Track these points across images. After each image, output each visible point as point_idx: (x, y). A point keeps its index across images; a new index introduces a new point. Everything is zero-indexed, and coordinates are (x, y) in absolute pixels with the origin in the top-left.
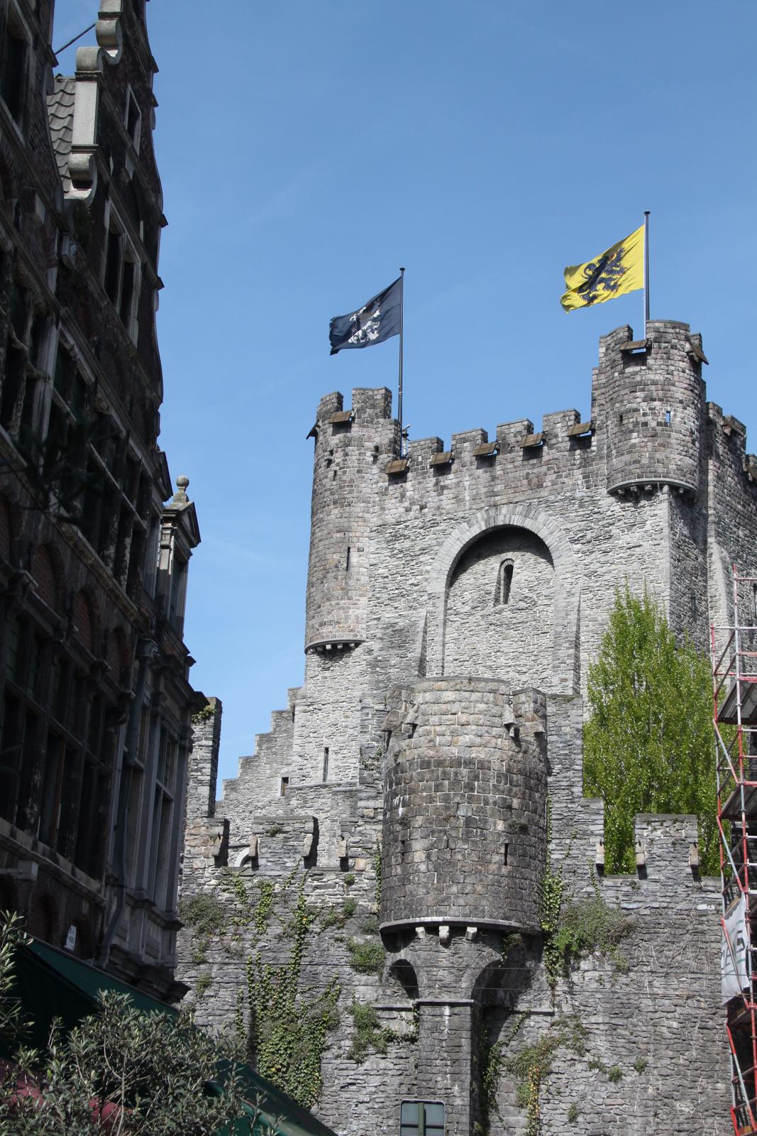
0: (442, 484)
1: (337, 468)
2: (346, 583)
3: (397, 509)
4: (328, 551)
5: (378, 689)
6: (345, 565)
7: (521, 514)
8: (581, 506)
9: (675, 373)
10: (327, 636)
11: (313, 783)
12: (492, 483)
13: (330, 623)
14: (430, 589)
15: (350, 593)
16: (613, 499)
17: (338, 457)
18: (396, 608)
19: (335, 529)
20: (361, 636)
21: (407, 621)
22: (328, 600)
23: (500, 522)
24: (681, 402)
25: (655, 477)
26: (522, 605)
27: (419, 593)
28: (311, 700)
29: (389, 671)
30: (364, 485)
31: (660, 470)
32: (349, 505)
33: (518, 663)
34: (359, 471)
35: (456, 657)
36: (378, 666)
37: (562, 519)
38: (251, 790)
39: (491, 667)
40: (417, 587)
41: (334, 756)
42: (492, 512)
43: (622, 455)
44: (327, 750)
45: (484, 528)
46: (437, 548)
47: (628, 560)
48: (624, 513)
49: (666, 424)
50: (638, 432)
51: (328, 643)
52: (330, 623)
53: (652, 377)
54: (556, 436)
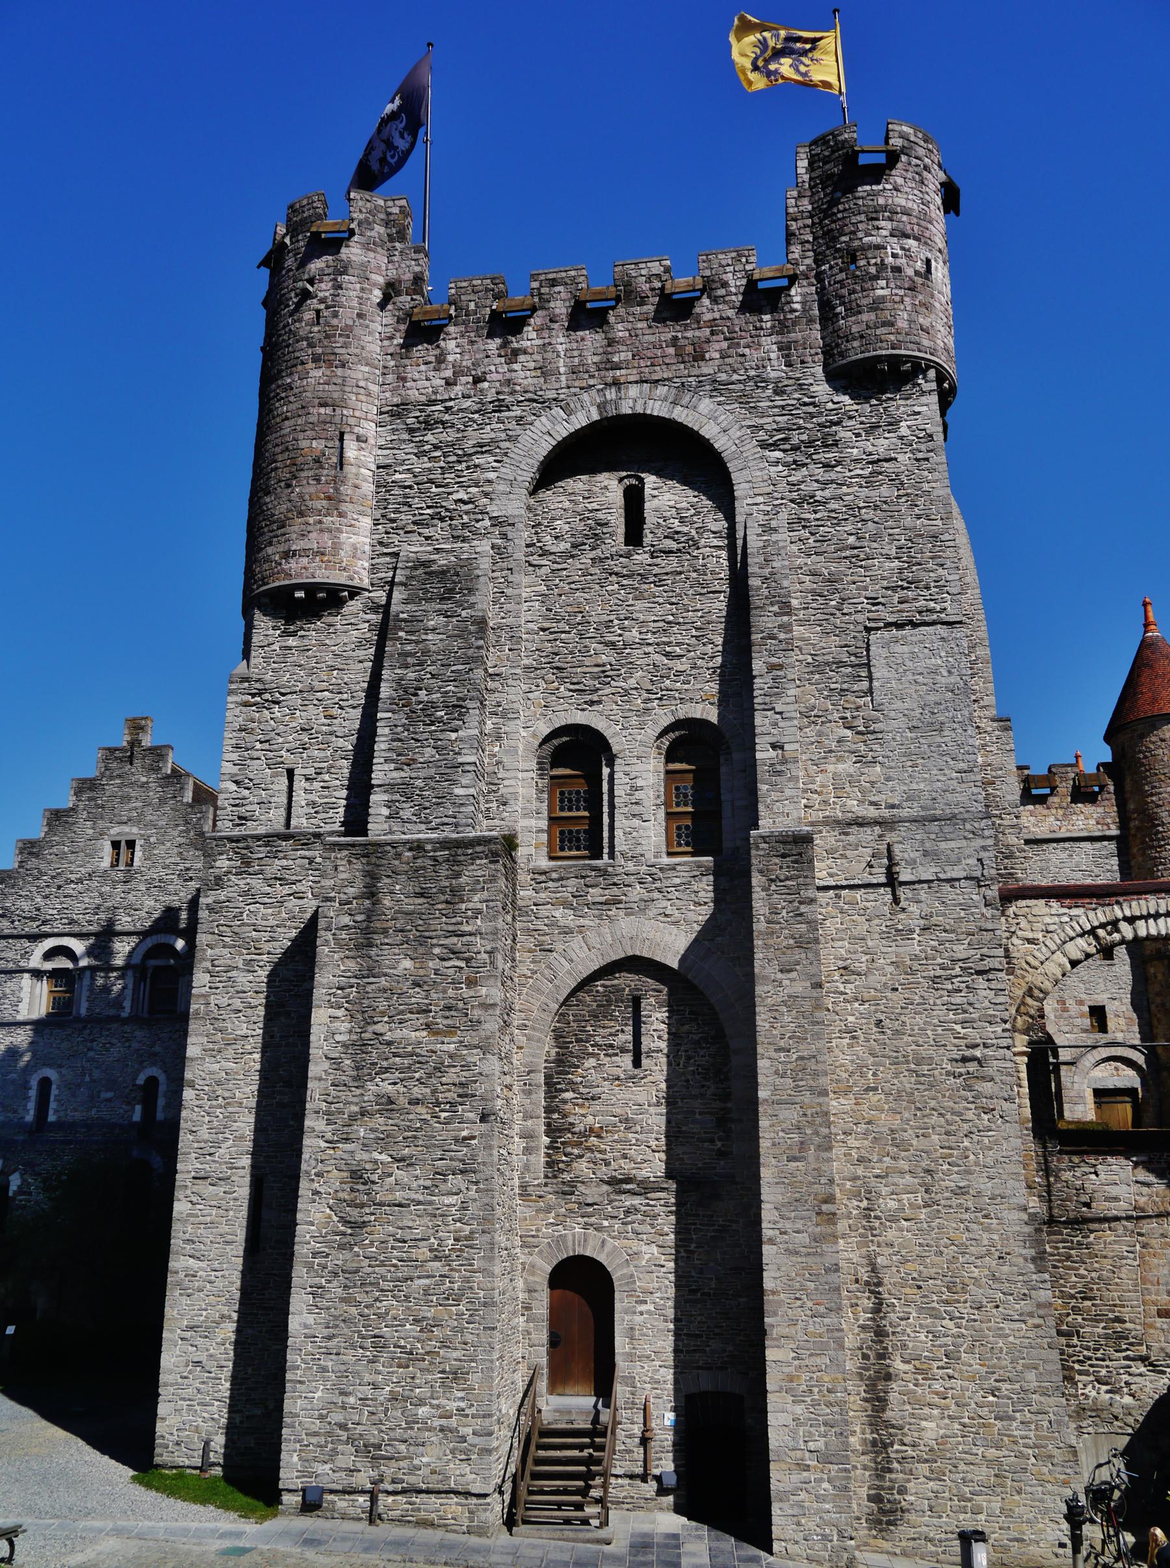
0: (515, 345)
2: (337, 490)
3: (428, 379)
4: (301, 435)
5: (406, 666)
6: (335, 460)
7: (665, 399)
8: (776, 393)
11: (261, 830)
12: (609, 349)
13: (305, 552)
15: (344, 507)
18: (427, 538)
19: (317, 401)
21: (453, 559)
22: (301, 514)
25: (920, 351)
26: (670, 544)
27: (472, 516)
28: (258, 685)
29: (424, 637)
30: (370, 339)
32: (343, 366)
33: (664, 639)
34: (360, 316)
35: (546, 625)
36: (402, 629)
37: (743, 411)
38: (61, 856)
39: (613, 644)
40: (471, 506)
41: (307, 785)
42: (611, 394)
44: (290, 773)
45: (595, 416)
46: (507, 444)
47: (870, 482)
50: (887, 280)
51: (299, 587)
52: (305, 552)
53: (903, 202)
54: (725, 285)
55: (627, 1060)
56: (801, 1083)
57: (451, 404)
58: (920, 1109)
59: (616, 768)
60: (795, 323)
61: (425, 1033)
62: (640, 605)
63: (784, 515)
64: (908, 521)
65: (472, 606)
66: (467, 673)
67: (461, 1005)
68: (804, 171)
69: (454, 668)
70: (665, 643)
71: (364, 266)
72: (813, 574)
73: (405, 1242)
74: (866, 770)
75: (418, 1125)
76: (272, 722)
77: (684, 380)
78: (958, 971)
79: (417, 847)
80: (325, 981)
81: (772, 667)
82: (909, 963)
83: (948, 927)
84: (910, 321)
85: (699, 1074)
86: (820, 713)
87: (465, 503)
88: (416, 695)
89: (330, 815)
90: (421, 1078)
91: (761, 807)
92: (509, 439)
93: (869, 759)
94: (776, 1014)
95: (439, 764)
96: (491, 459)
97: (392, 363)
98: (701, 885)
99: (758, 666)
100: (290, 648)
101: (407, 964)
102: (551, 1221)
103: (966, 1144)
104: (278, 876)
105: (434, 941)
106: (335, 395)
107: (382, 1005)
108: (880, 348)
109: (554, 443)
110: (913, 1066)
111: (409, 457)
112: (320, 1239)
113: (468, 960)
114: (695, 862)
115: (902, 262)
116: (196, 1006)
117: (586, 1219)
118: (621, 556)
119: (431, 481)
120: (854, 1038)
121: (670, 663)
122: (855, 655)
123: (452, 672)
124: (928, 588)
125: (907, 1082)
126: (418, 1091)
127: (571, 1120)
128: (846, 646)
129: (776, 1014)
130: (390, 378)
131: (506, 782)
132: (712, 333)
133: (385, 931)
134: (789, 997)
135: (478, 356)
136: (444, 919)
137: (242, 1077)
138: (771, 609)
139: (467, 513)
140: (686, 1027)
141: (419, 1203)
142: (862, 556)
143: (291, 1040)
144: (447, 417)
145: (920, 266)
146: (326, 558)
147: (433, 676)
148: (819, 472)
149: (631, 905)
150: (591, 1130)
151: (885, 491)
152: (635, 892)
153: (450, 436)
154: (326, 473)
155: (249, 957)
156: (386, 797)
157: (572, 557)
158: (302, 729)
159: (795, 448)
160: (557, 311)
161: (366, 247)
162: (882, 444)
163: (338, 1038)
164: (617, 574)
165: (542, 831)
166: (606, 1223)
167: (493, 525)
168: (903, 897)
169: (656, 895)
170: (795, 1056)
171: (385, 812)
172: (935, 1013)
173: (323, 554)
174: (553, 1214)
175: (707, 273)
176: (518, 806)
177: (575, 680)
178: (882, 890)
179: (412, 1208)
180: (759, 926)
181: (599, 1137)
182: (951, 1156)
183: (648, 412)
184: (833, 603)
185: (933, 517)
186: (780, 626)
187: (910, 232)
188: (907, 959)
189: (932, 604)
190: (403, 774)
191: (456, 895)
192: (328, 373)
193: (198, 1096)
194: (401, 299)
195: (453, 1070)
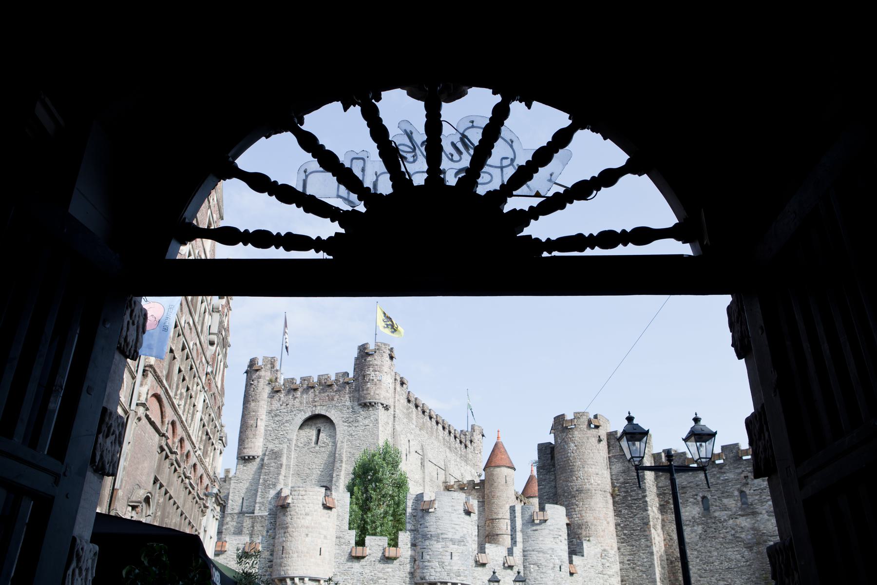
1: (255, 387)
5: (265, 475)
6: (255, 425)
9: (385, 362)
14: (288, 437)
23: (317, 413)
24: (386, 372)
31: (377, 397)
34: (263, 389)
39: (309, 469)
42: (314, 409)
45: (310, 414)
46: (291, 421)
49: (380, 381)
51: (246, 456)
54: (340, 381)
63: (346, 439)
64: (370, 440)
65: (280, 461)
71: (264, 376)
72: (350, 453)
81: (337, 475)
92: (293, 419)
99: (334, 475)
119: (276, 430)
130: (269, 404)
147: (271, 478)
148: (354, 428)
153: (280, 418)
154: (254, 428)
156: (259, 505)
159: (350, 422)
162: (367, 422)
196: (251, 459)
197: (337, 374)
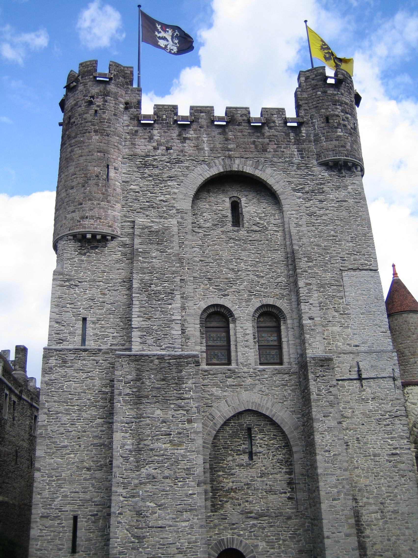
0: (184, 136)
2: (106, 190)
4: (89, 164)
6: (105, 177)
8: (297, 168)
10: (89, 227)
12: (226, 142)
13: (92, 217)
16: (323, 168)
17: (99, 101)
18: (147, 216)
20: (117, 232)
22: (90, 200)
23: (235, 168)
28: (67, 277)
29: (152, 261)
30: (118, 125)
32: (108, 136)
33: (255, 269)
35: (202, 259)
39: (233, 269)
40: (166, 203)
41: (92, 326)
42: (227, 161)
43: (332, 140)
44: (84, 320)
45: (222, 170)
46: (182, 178)
47: (338, 208)
48: (330, 178)
51: (89, 232)
52: (92, 217)
54: (274, 122)
55: (246, 457)
56: (336, 466)
57: (157, 157)
58: (376, 476)
59: (237, 325)
60: (304, 141)
61: (168, 445)
62: (243, 253)
63: (304, 219)
66: (174, 278)
67: (185, 432)
68: (303, 82)
69: (167, 276)
70: (255, 270)
71: (116, 94)
73: (164, 545)
74: (345, 330)
75: (168, 489)
76: (75, 295)
77: (259, 159)
78: (387, 416)
79: (161, 358)
80: (119, 420)
81: (307, 284)
82: (368, 413)
83: (383, 398)
84: (351, 146)
85: (278, 462)
86: (324, 305)
87: (164, 201)
88: (150, 287)
89: (105, 340)
90: (168, 466)
91: (307, 345)
92: (183, 175)
93: (346, 325)
94: (323, 435)
95: (164, 319)
96: (175, 183)
97: (128, 137)
98: (277, 378)
99: (301, 283)
100: (83, 261)
101: (158, 412)
102: (217, 532)
103: (396, 491)
104: (81, 368)
105: (171, 402)
106: (105, 148)
107: (148, 432)
108: (341, 156)
109: (204, 179)
110: (372, 457)
111: (137, 179)
112: (123, 545)
113: (187, 411)
114: (274, 368)
115: (346, 123)
116: (40, 431)
117: (233, 531)
118: (235, 231)
120: (347, 445)
121: (259, 280)
122: (337, 281)
123: (166, 277)
124: (364, 255)
125: (371, 464)
126: (167, 473)
127: (222, 485)
128: (333, 277)
129: (323, 435)
131: (189, 329)
132: (270, 141)
133: (147, 397)
134: (328, 428)
135: (168, 138)
136: (175, 392)
137: (65, 466)
138: (304, 259)
139: (165, 206)
140: (272, 442)
141: (170, 526)
142: (337, 240)
143: (89, 448)
144: (154, 163)
145: (352, 125)
146: (102, 221)
147: (158, 279)
149: (246, 387)
150: (232, 489)
151: (345, 214)
152: (248, 381)
153: (157, 171)
155: (67, 407)
156: (139, 333)
157: (213, 229)
158: (90, 299)
159: (307, 193)
160: (202, 123)
161: (117, 85)
162: (342, 194)
163: (127, 447)
164: (233, 239)
165: (203, 352)
166: (242, 533)
167: (177, 213)
168: (364, 384)
169: (257, 382)
170: (332, 454)
171: (139, 340)
172: (380, 434)
173: (100, 219)
174: (217, 529)
175: (266, 116)
176: (192, 340)
177: (217, 284)
178: (355, 382)
179: (167, 528)
180: (314, 397)
181: (235, 492)
182: (390, 496)
183: (244, 171)
184: (327, 259)
185: (364, 226)
186: (308, 267)
187: (348, 112)
188: (367, 411)
189: (366, 262)
190: (147, 323)
191: (180, 381)
192: (101, 138)
193: (43, 476)
194: (132, 110)
195: (183, 462)
196: (99, 241)
197: (264, 111)
